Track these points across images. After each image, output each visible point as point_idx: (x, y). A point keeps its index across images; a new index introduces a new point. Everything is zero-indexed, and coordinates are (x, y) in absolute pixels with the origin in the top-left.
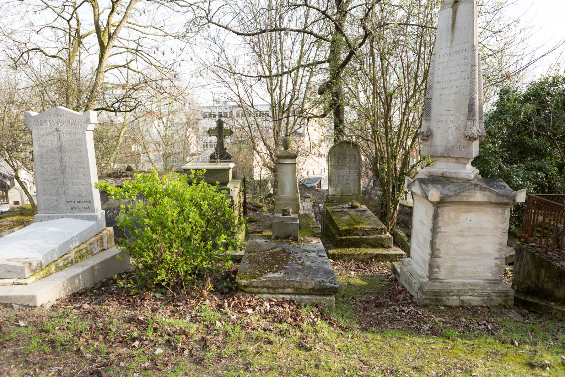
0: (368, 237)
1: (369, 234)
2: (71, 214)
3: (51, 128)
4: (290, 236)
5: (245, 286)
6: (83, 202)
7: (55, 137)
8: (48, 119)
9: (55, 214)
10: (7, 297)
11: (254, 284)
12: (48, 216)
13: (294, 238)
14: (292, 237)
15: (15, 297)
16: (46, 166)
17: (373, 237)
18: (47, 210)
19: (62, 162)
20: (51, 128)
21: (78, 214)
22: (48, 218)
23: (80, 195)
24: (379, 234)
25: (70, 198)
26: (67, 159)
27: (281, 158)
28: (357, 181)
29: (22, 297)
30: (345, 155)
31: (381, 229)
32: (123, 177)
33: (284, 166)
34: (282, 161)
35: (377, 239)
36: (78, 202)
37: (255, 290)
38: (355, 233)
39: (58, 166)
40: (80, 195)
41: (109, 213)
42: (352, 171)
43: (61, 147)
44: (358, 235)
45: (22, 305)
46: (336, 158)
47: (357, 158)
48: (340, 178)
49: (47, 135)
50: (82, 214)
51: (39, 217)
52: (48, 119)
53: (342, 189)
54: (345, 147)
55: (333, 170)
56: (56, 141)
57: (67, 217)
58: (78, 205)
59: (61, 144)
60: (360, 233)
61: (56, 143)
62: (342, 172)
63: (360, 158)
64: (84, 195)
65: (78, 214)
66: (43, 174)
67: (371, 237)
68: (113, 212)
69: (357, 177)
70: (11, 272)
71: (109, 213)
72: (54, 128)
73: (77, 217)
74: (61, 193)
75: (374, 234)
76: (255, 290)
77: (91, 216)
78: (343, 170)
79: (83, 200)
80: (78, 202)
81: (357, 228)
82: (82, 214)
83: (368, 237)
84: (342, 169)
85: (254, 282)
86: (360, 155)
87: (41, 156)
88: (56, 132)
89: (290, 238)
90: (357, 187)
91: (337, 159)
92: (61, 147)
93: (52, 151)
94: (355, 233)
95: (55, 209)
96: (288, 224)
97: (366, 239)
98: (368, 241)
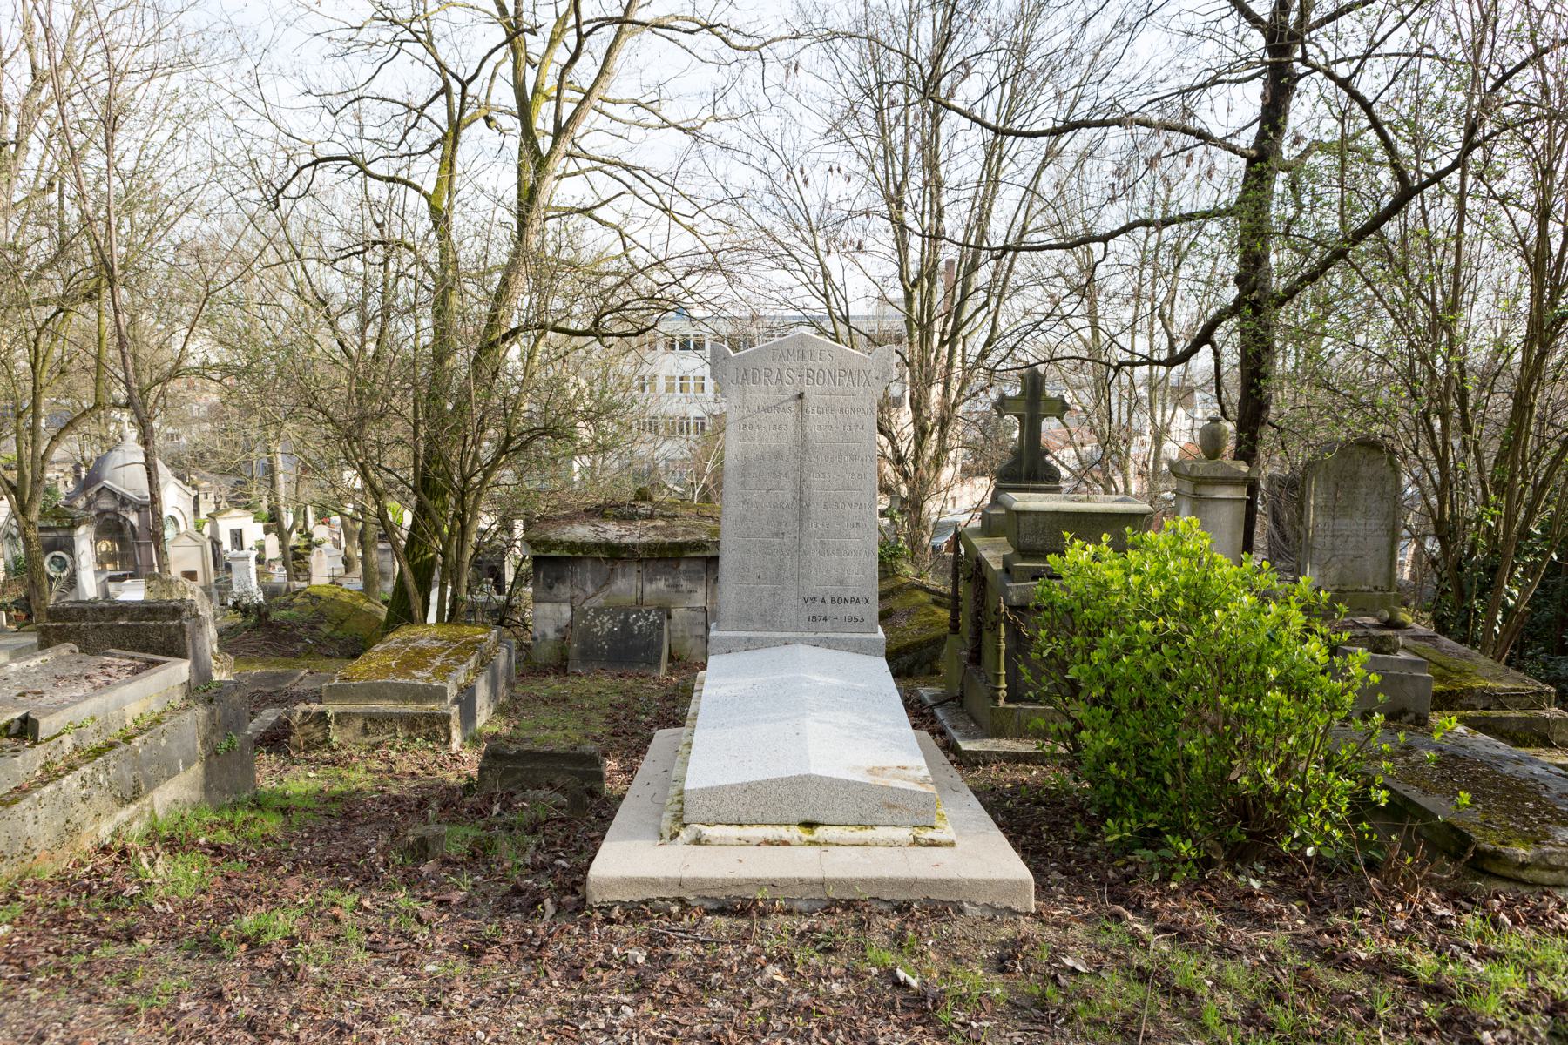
0: (1502, 713)
1: (1503, 707)
2: (812, 635)
3: (781, 391)
4: (1404, 712)
5: (1524, 866)
6: (846, 601)
7: (789, 418)
8: (774, 366)
9: (768, 634)
10: (948, 882)
11: (1552, 861)
12: (749, 639)
13: (1418, 717)
14: (1411, 716)
15: (973, 882)
16: (755, 497)
17: (1518, 714)
18: (744, 620)
19: (801, 487)
20: (781, 391)
21: (832, 635)
22: (749, 645)
23: (841, 582)
24: (1532, 706)
25: (813, 589)
26: (815, 482)
27: (1206, 484)
28: (1384, 552)
29: (990, 883)
30: (1355, 477)
31: (1540, 694)
32: (641, 517)
33: (1211, 506)
34: (1207, 492)
35: (1530, 722)
36: (833, 601)
37: (1548, 877)
38: (1464, 702)
39: (789, 497)
40: (841, 582)
41: (636, 620)
42: (1374, 523)
43: (802, 444)
44: (1473, 707)
45: (991, 907)
46: (1331, 484)
47: (1388, 488)
48: (1338, 542)
49: (769, 409)
50: (839, 636)
51: (722, 641)
52: (774, 366)
53: (1341, 575)
54: (1356, 456)
55: (1319, 520)
56: (792, 428)
57: (803, 641)
58: (832, 610)
59: (803, 436)
60: (1480, 703)
61: (790, 434)
62: (1344, 524)
63: (1398, 488)
64: (851, 581)
65: (832, 635)
66: (744, 519)
67: (1512, 715)
68: (647, 619)
69: (1385, 541)
70: (894, 807)
71: (636, 620)
72: (792, 390)
73: (830, 644)
74: (787, 574)
75: (1517, 706)
76: (1548, 877)
77: (868, 641)
78: (1347, 520)
79: (849, 596)
80: (833, 601)
81: (1471, 690)
82: (839, 636)
83: (1502, 713)
84: (1345, 515)
85: (1551, 853)
86: (1398, 480)
87: (744, 470)
88: (792, 403)
89: (1405, 719)
90: (1384, 569)
91: (1332, 489)
92: (802, 444)
93: (778, 455)
94: (1464, 702)
95: (768, 619)
96: (1402, 679)
97: (1501, 719)
98: (1505, 727)
